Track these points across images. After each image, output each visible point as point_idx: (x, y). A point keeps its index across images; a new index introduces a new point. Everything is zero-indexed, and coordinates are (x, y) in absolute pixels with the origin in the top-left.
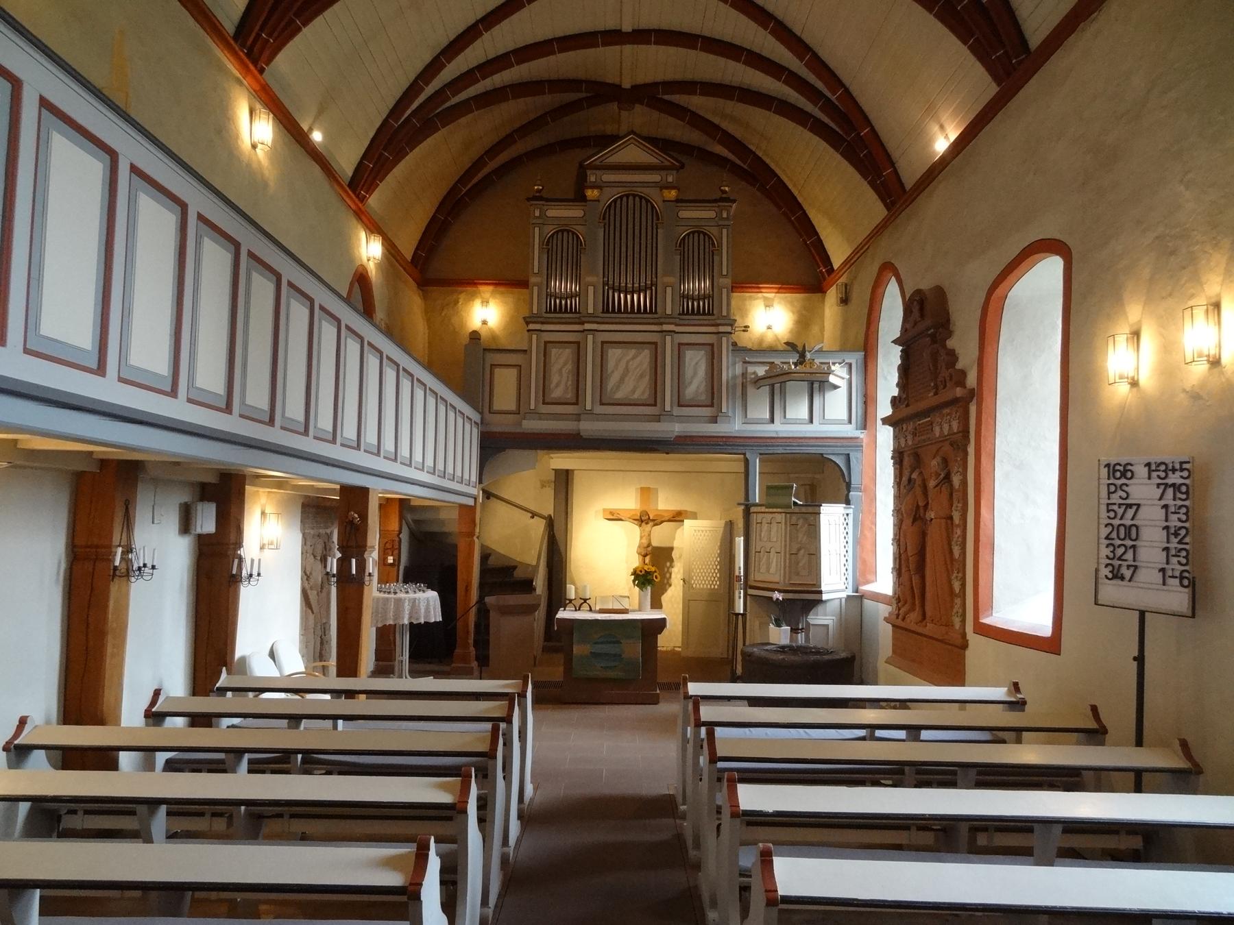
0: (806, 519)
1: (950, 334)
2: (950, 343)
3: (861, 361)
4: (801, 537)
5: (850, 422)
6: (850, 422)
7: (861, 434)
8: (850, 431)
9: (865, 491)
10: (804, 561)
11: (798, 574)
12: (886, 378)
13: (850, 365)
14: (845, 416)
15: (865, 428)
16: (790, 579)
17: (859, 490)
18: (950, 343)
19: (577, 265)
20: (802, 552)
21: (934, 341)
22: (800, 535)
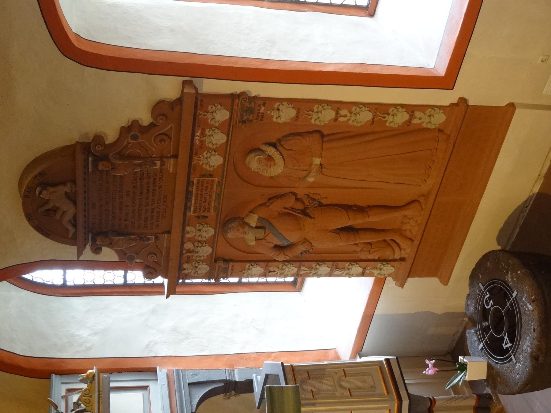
0: (303, 382)
1: (98, 139)
2: (111, 136)
3: (65, 379)
4: (326, 385)
5: (146, 388)
6: (146, 388)
7: (162, 373)
8: (158, 389)
9: (232, 366)
10: (355, 382)
11: (373, 387)
12: (89, 349)
13: (69, 391)
14: (138, 395)
15: (153, 371)
16: (383, 395)
17: (232, 372)
18: (111, 136)
19: (196, 98)
20: (344, 384)
21: (105, 158)
22: (324, 387)
